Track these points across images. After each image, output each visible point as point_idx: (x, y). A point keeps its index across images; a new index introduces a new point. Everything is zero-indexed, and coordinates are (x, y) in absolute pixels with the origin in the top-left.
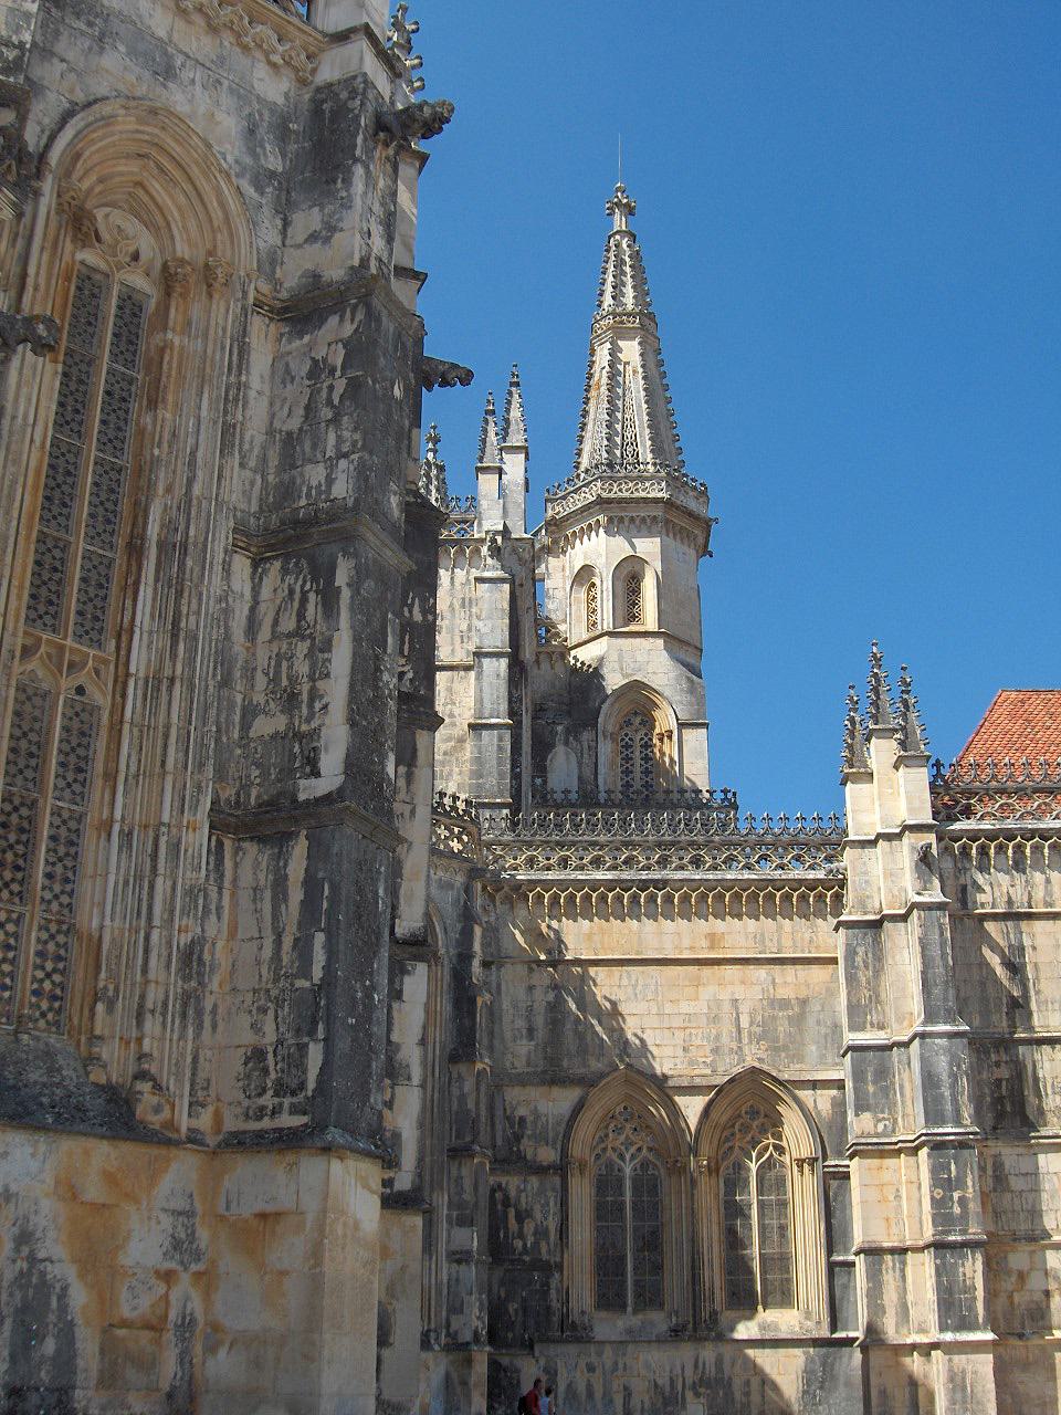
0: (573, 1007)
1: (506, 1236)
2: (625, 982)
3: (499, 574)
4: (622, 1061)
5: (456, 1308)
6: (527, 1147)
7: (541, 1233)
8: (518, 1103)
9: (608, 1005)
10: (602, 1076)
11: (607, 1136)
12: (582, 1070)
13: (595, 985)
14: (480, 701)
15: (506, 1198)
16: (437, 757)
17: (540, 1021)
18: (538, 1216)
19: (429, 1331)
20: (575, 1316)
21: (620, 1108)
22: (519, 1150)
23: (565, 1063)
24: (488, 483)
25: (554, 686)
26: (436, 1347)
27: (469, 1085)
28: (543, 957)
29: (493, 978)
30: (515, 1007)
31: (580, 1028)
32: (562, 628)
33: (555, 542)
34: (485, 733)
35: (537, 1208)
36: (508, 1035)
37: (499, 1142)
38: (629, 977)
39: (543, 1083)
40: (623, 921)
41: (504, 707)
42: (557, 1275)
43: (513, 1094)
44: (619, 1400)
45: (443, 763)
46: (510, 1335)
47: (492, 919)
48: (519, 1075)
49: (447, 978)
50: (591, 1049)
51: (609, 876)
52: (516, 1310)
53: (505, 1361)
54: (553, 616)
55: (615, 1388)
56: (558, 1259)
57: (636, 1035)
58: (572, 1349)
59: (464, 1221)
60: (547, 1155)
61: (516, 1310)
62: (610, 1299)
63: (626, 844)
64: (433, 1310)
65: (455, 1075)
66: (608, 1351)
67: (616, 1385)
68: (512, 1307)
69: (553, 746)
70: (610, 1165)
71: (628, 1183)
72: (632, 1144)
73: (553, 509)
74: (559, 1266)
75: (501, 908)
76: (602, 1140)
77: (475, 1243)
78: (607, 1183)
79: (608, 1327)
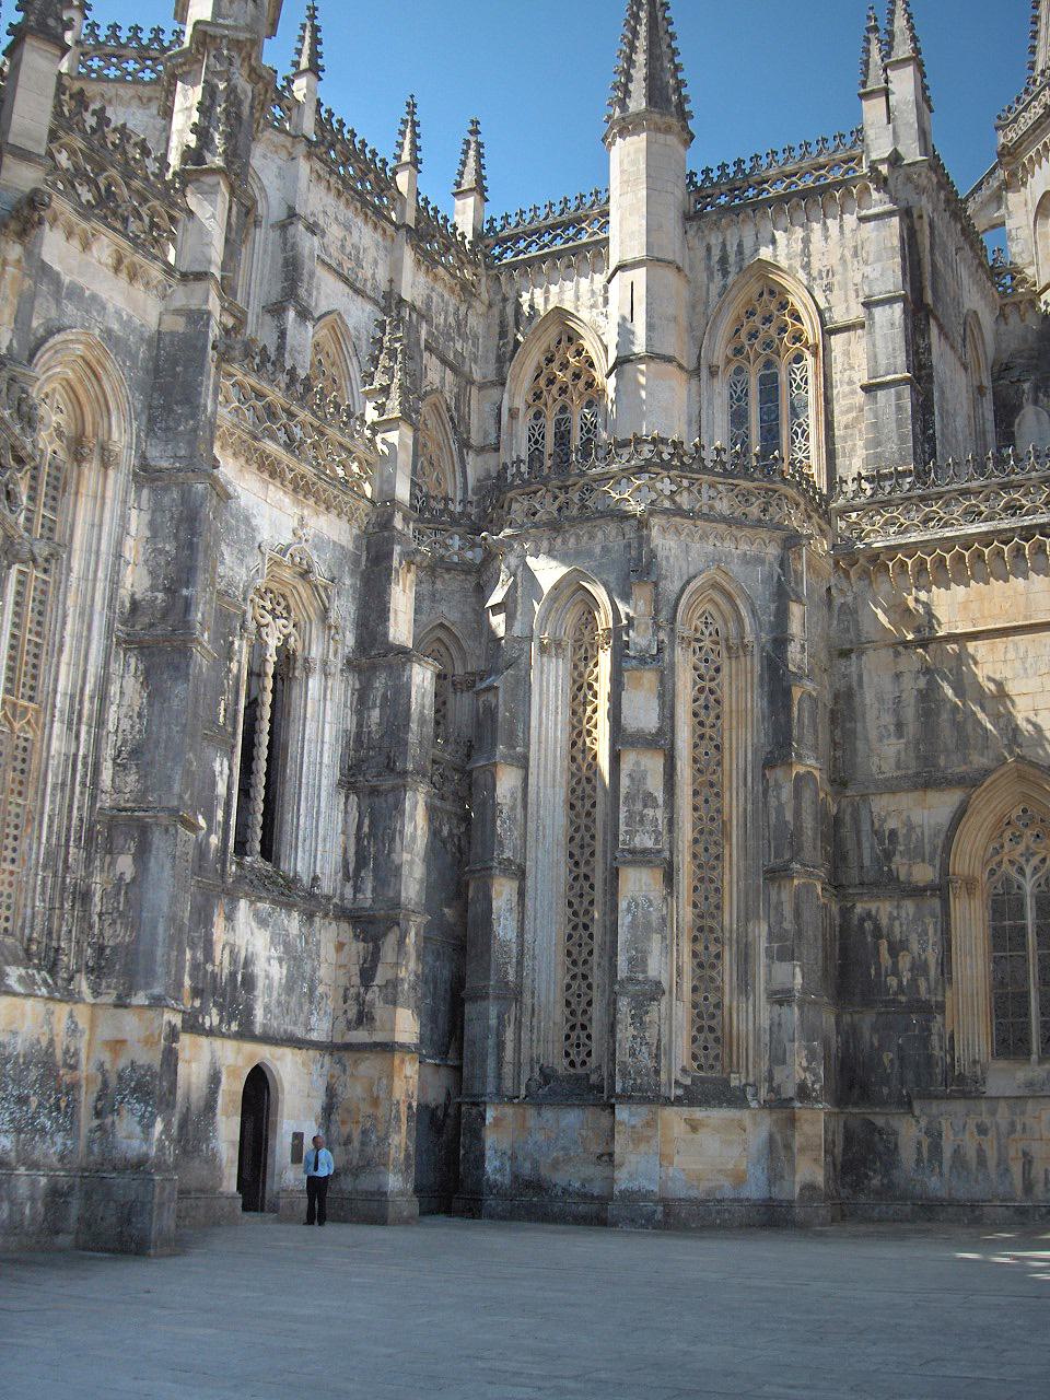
0: (949, 692)
1: (878, 974)
2: (1011, 655)
3: (889, 207)
4: (1011, 752)
5: (778, 1058)
6: (900, 865)
7: (919, 968)
8: (889, 814)
9: (992, 687)
10: (987, 772)
11: (1002, 847)
12: (963, 768)
13: (976, 663)
14: (873, 358)
15: (877, 929)
16: (837, 433)
17: (910, 713)
18: (915, 947)
19: (747, 1084)
20: (963, 1066)
21: (1018, 811)
22: (890, 870)
23: (942, 762)
24: (873, 110)
25: (1025, 340)
26: (754, 1104)
27: (786, 793)
28: (910, 637)
29: (853, 669)
30: (881, 700)
31: (959, 717)
32: (1030, 271)
33: (1013, 174)
34: (880, 394)
35: (914, 938)
36: (873, 734)
37: (867, 862)
38: (1017, 650)
39: (915, 788)
40: (1006, 581)
41: (901, 359)
42: (939, 1018)
43: (881, 804)
44: (1016, 1169)
45: (844, 439)
46: (885, 1090)
47: (850, 599)
48: (887, 780)
49: (758, 668)
50: (972, 742)
51: (984, 527)
52: (891, 1061)
53: (880, 1121)
54: (1018, 261)
55: (1012, 1153)
56: (940, 999)
57: (1029, 721)
58: (958, 1106)
59: (785, 954)
60: (924, 873)
61: (891, 1061)
62: (1011, 1044)
63: (1005, 487)
64: (751, 1059)
65: (772, 783)
66: (1003, 1108)
67: (1013, 1152)
68: (887, 1057)
69: (1020, 407)
70: (1008, 881)
71: (1029, 903)
72: (1033, 855)
73: (1005, 136)
74: (941, 1007)
75: (858, 586)
76: (996, 852)
77: (799, 980)
78: (1004, 906)
79: (1004, 1079)
